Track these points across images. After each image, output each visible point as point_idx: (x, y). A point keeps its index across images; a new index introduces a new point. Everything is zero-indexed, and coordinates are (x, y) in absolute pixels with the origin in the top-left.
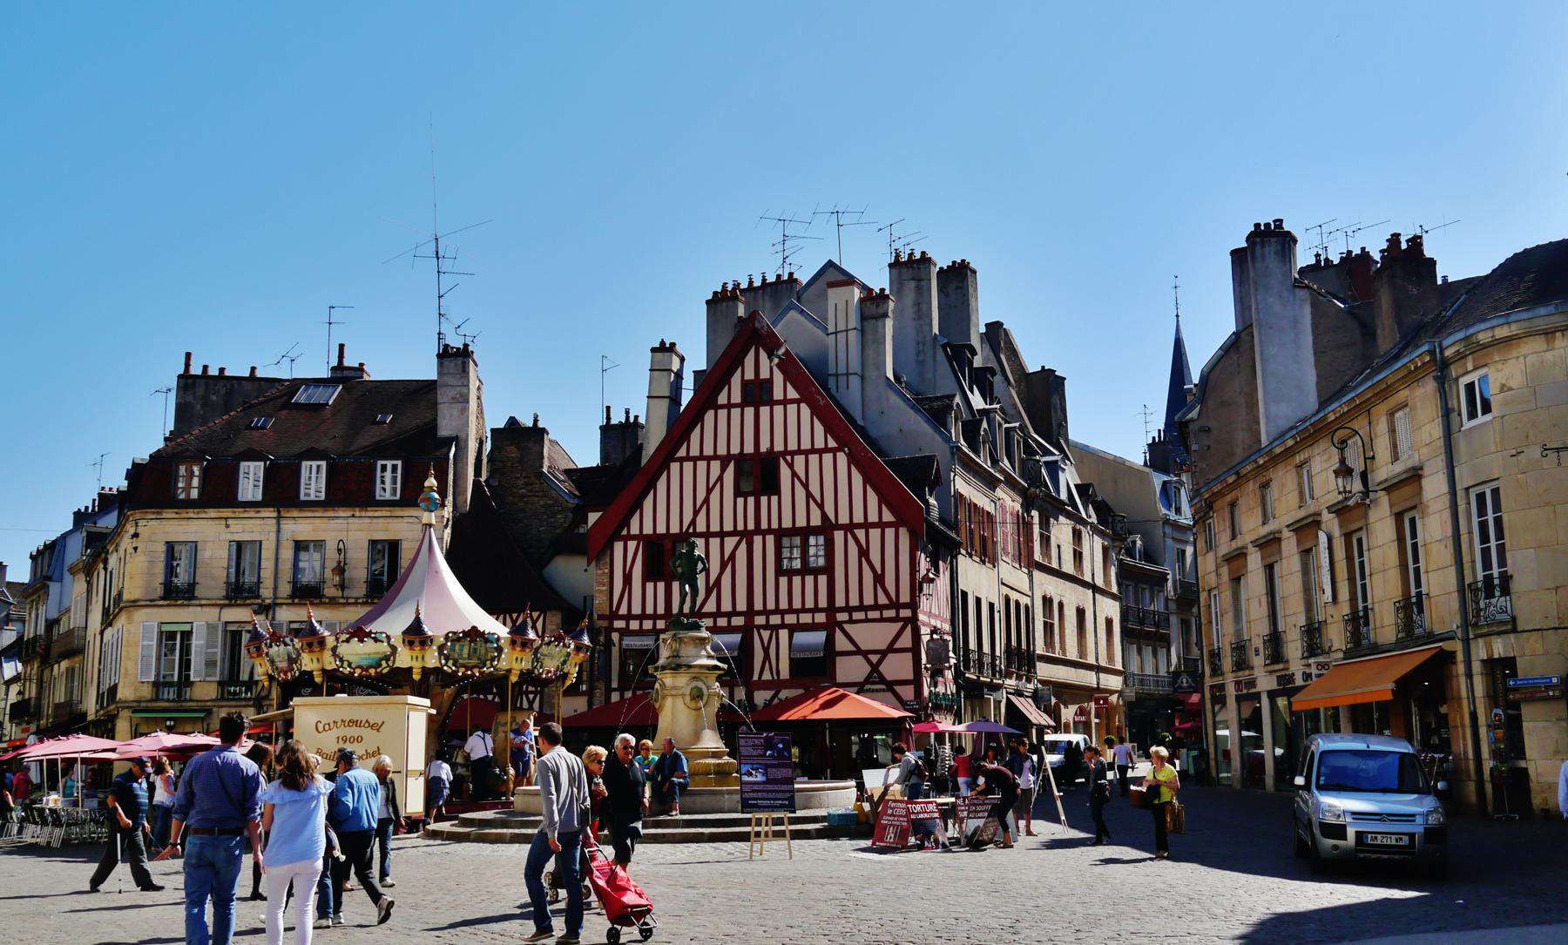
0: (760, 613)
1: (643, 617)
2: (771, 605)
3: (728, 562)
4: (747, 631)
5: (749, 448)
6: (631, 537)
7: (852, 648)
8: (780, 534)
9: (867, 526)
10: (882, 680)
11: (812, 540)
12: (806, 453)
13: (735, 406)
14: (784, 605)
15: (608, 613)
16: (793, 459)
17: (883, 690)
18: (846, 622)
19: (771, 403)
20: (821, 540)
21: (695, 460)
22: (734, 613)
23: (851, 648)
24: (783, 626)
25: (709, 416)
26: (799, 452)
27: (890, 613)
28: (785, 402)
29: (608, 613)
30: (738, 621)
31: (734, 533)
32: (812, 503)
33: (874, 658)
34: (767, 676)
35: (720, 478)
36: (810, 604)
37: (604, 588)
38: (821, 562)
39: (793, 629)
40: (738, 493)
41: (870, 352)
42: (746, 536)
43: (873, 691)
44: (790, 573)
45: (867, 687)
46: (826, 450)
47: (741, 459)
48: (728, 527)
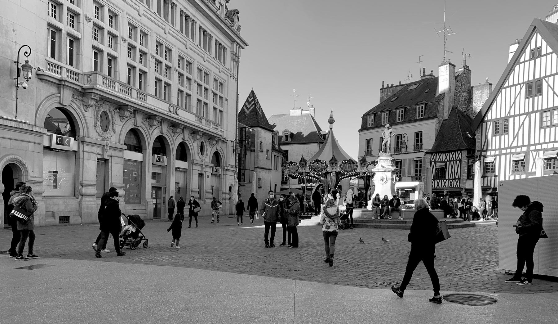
3: (522, 125)
8: (543, 111)
13: (527, 61)
15: (480, 150)
19: (540, 56)
24: (541, 150)
25: (517, 68)
28: (546, 55)
29: (480, 150)
35: (520, 92)
37: (479, 141)
40: (526, 98)
42: (528, 114)
48: (522, 112)
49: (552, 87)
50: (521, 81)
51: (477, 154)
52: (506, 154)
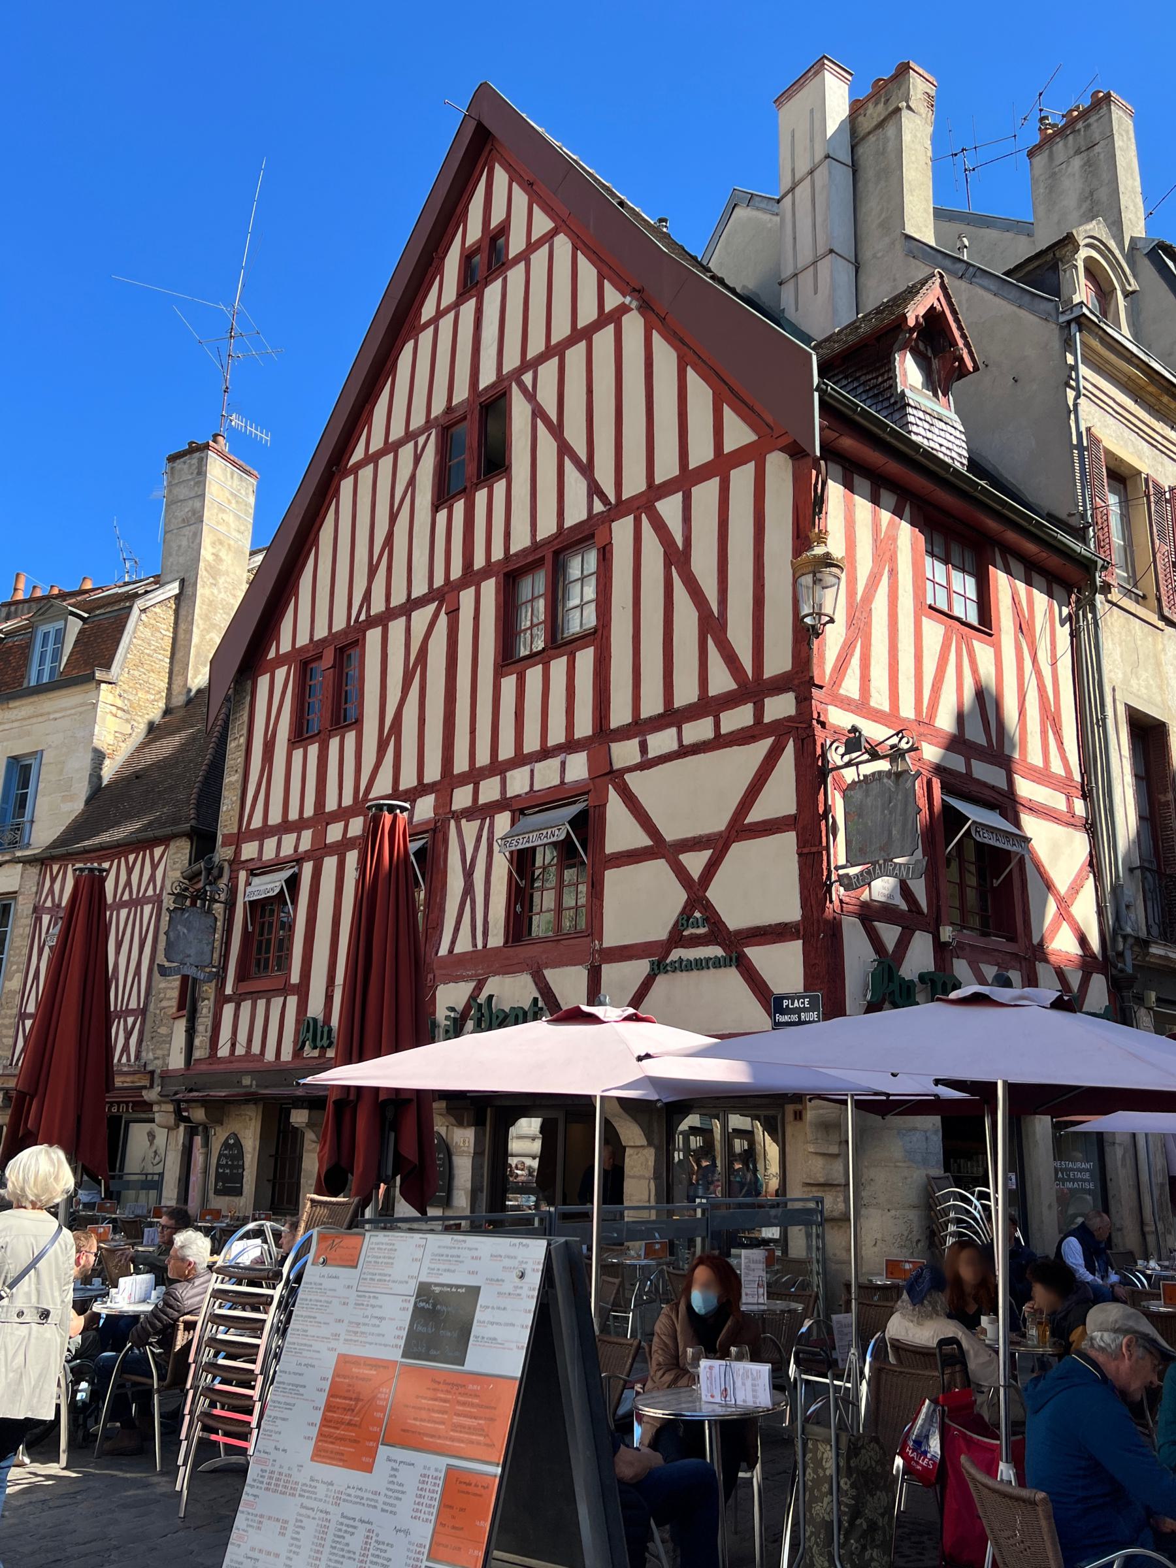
1: (286, 827)
3: (417, 665)
6: (281, 660)
23: (644, 841)
32: (568, 464)
40: (436, 508)
41: (872, 206)
48: (419, 589)
50: (418, 421)
51: (223, 853)
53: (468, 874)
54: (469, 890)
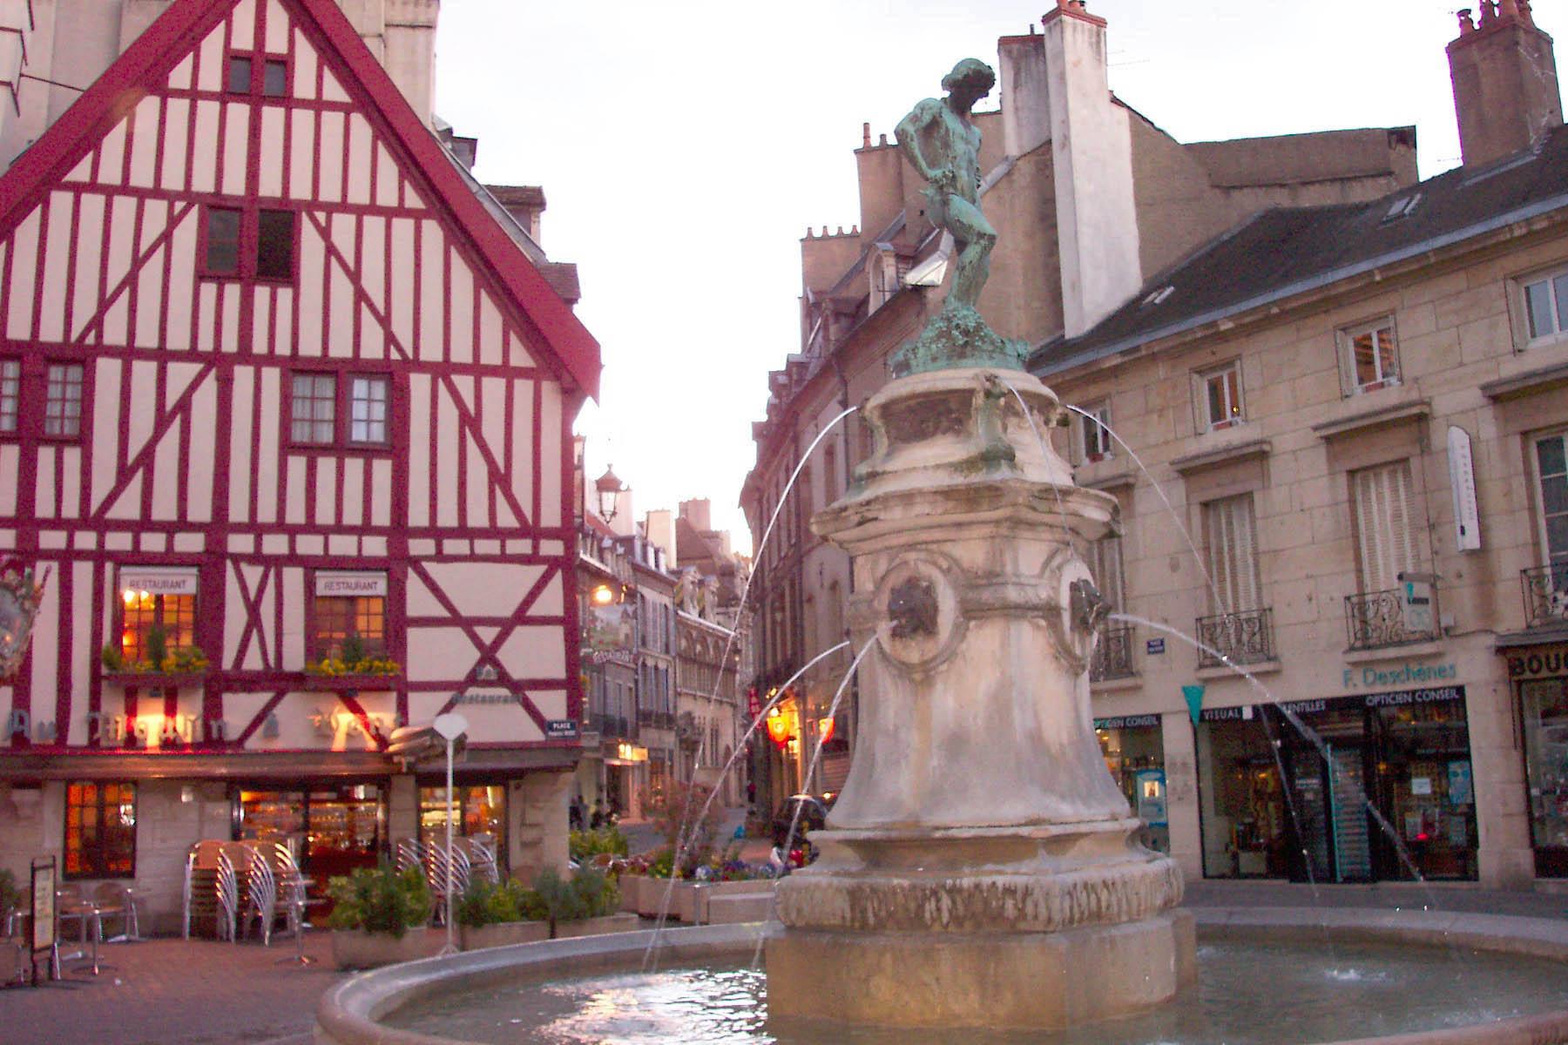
0: (239, 528)
2: (267, 514)
4: (211, 565)
5: (235, 185)
7: (445, 614)
8: (295, 367)
9: (477, 370)
10: (503, 679)
11: (360, 387)
12: (360, 211)
14: (296, 515)
16: (329, 220)
17: (506, 700)
18: (429, 558)
19: (287, 101)
20: (379, 390)
21: (110, 192)
22: (182, 524)
23: (445, 614)
26: (344, 206)
27: (521, 546)
30: (190, 543)
31: (192, 355)
32: (365, 311)
33: (488, 634)
34: (253, 662)
35: (166, 237)
36: (353, 516)
38: (378, 434)
39: (311, 565)
40: (201, 277)
42: (218, 363)
43: (484, 700)
44: (312, 451)
45: (472, 691)
46: (401, 211)
47: (215, 205)
49: (351, 264)
52: (67, 558)
53: (253, 609)
54: (254, 620)
